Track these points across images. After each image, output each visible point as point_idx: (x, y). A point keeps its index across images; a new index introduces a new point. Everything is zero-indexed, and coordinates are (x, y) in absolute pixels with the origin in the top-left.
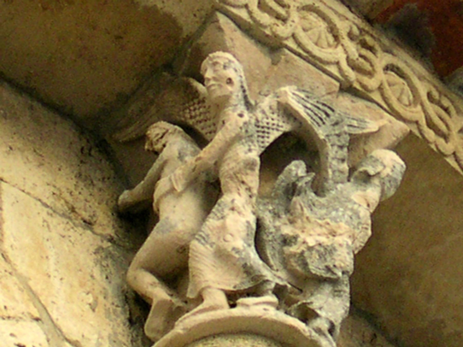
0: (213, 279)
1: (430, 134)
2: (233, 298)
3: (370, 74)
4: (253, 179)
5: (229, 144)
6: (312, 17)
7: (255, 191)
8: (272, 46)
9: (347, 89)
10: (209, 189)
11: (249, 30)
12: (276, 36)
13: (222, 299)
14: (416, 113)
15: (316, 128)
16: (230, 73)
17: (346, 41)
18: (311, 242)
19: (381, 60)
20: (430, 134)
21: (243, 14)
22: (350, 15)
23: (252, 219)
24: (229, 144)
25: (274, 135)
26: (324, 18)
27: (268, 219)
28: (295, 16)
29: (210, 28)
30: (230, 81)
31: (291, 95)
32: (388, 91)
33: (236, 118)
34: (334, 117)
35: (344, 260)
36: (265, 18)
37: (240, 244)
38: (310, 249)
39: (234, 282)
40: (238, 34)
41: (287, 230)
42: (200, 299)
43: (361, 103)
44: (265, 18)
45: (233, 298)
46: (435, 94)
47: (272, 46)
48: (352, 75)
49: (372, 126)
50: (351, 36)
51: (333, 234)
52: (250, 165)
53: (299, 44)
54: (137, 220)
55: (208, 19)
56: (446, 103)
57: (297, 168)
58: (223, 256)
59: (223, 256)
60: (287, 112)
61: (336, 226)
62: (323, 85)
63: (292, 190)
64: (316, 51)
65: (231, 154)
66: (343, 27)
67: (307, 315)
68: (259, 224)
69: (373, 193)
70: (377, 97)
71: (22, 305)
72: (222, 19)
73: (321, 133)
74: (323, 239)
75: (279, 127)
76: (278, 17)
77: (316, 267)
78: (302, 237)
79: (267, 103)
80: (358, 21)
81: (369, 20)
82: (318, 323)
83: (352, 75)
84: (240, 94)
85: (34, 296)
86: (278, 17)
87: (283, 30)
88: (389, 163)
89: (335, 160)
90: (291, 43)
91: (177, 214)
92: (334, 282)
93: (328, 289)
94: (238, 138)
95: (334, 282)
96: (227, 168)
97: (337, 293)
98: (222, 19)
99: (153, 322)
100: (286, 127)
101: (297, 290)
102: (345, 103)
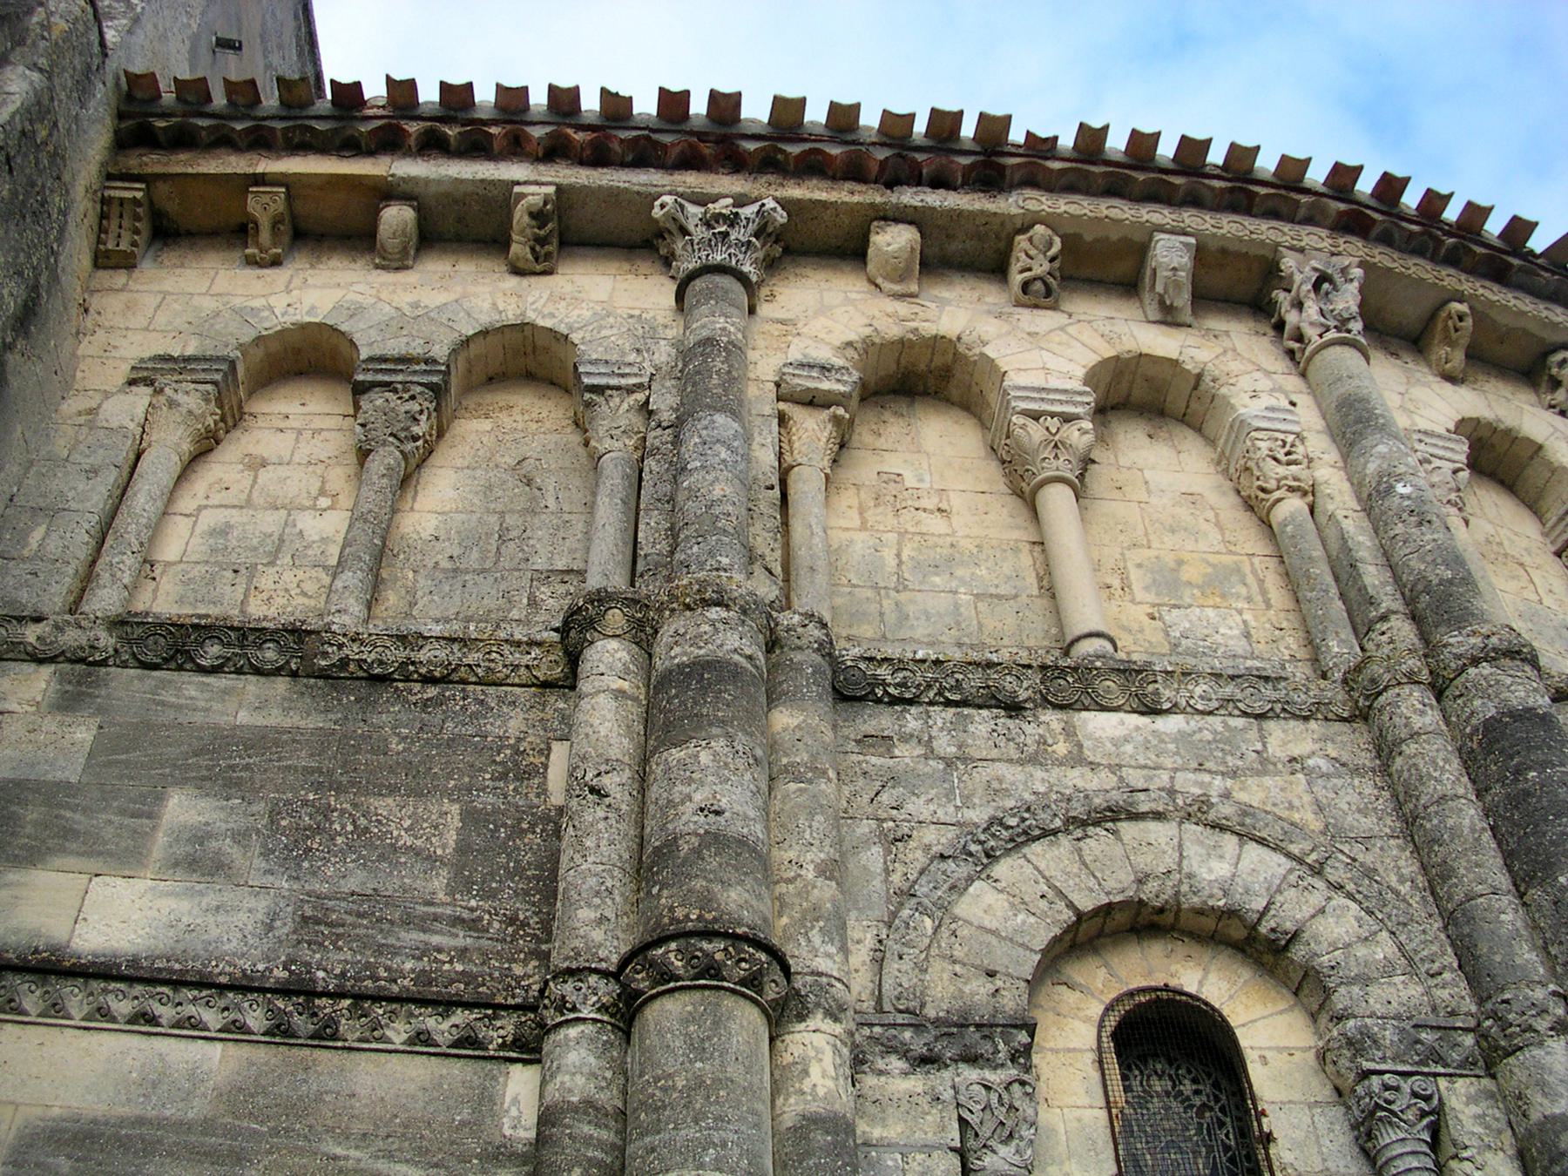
0: (1311, 333)
2: (1321, 336)
4: (1312, 295)
8: (1301, 250)
9: (1333, 254)
10: (1299, 305)
11: (1291, 248)
19: (1341, 241)
31: (1314, 263)
33: (1298, 278)
35: (1355, 309)
45: (1321, 336)
47: (1301, 250)
54: (1280, 326)
55: (1276, 251)
57: (1326, 286)
58: (1312, 324)
59: (1312, 324)
60: (1315, 269)
61: (1347, 299)
62: (1324, 256)
63: (1327, 294)
67: (1349, 331)
69: (1356, 284)
71: (1251, 367)
75: (1315, 276)
77: (1346, 315)
79: (1307, 269)
88: (1357, 272)
91: (1292, 318)
99: (1298, 356)
101: (1343, 324)
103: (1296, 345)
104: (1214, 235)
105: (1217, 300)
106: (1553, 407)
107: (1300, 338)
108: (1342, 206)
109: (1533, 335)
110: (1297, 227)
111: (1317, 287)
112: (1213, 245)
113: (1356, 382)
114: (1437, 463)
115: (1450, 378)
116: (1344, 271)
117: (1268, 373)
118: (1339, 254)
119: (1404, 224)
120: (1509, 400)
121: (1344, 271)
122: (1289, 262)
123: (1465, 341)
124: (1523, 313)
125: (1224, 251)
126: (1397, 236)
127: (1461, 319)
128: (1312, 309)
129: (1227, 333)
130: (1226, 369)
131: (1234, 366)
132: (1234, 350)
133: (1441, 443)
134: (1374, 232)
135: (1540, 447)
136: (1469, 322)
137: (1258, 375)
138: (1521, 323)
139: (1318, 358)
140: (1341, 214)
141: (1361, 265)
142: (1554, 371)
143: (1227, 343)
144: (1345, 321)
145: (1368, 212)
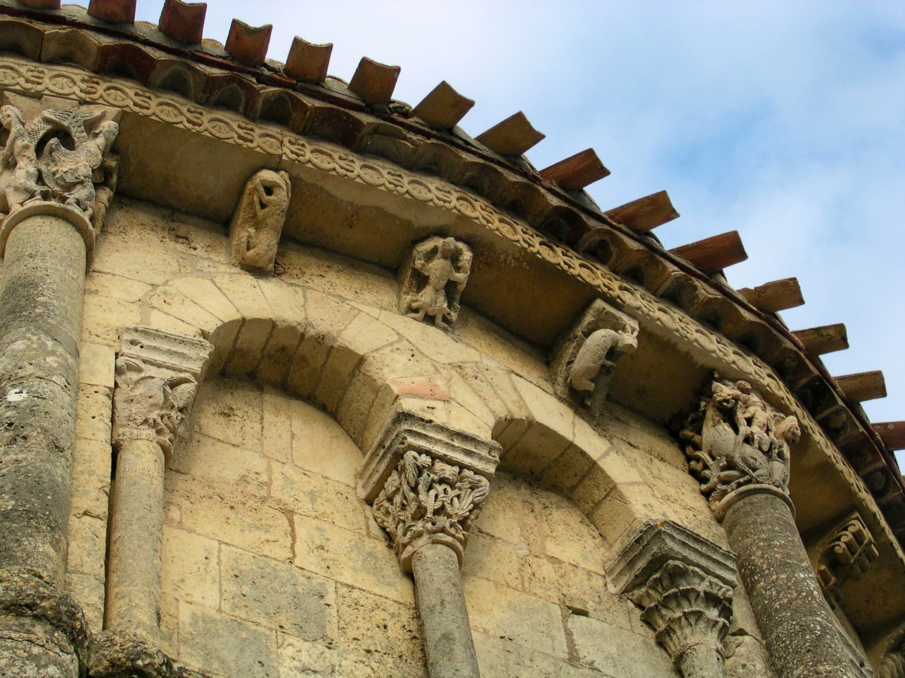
1: (137, 109)
3: (95, 93)
4: (31, 153)
5: (14, 142)
6: (59, 79)
8: (38, 96)
9: (83, 102)
11: (24, 93)
12: (37, 91)
15: (62, 122)
16: (9, 112)
17: (79, 83)
18: (65, 170)
20: (137, 109)
21: (18, 87)
22: (83, 72)
23: (32, 170)
24: (14, 142)
25: (42, 133)
27: (43, 168)
28: (46, 80)
30: (9, 116)
31: (47, 114)
32: (106, 97)
34: (72, 115)
36: (29, 86)
37: (22, 181)
38: (65, 172)
40: (18, 96)
41: (54, 169)
43: (92, 107)
44: (29, 86)
45: (22, 204)
46: (141, 93)
47: (38, 96)
48: (83, 95)
50: (83, 81)
51: (77, 163)
52: (26, 147)
53: (51, 91)
56: (148, 95)
58: (17, 189)
59: (17, 189)
60: (47, 121)
66: (77, 78)
68: (40, 171)
69: (101, 140)
70: (101, 101)
72: (6, 93)
73: (66, 124)
74: (73, 167)
77: (70, 179)
78: (61, 169)
80: (90, 74)
81: (94, 72)
83: (83, 95)
84: (17, 120)
86: (39, 84)
87: (39, 88)
89: (77, 133)
90: (47, 92)
92: (82, 183)
93: (79, 187)
94: (16, 138)
95: (82, 183)
96: (16, 151)
97: (84, 187)
98: (6, 93)
100: (49, 127)
102: (84, 108)
106: (416, 311)
108: (106, 41)
109: (394, 217)
110: (42, 68)
113: (38, 262)
114: (151, 371)
115: (256, 270)
118: (93, 102)
119: (201, 67)
120: (342, 299)
123: (276, 220)
124: (370, 187)
127: (269, 191)
133: (165, 346)
134: (158, 76)
135: (362, 360)
136: (282, 197)
138: (370, 200)
140: (105, 51)
142: (418, 264)
144: (70, 187)
145: (148, 50)
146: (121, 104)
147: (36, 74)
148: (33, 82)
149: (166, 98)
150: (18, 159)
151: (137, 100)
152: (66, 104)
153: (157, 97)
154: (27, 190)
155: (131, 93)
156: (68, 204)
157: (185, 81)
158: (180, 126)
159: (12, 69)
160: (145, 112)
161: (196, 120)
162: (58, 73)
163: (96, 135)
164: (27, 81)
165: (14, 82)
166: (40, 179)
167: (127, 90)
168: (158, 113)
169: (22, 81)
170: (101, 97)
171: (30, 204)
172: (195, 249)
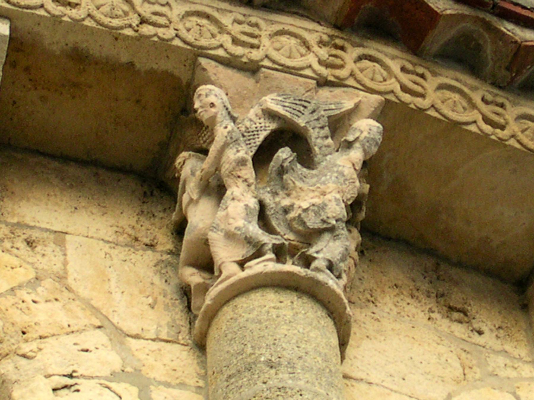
0: (225, 254)
1: (406, 98)
2: (242, 264)
3: (341, 67)
4: (248, 172)
5: (221, 152)
6: (283, 39)
7: (252, 180)
8: (252, 69)
9: (323, 83)
10: (215, 189)
11: (230, 63)
12: (252, 61)
13: (235, 268)
14: (393, 85)
15: (296, 119)
16: (212, 99)
17: (316, 48)
18: (305, 205)
19: (353, 53)
20: (406, 98)
21: (220, 52)
22: (319, 28)
23: (253, 203)
24: (221, 152)
25: (263, 135)
26: (295, 36)
27: (268, 199)
28: (265, 41)
29: (198, 71)
30: (212, 105)
31: (271, 102)
32: (360, 76)
33: (223, 130)
34: (310, 107)
35: (336, 210)
36: (239, 50)
37: (241, 223)
38: (306, 210)
39: (241, 252)
40: (221, 68)
41: (286, 202)
42: (221, 272)
43: (338, 91)
44: (239, 50)
45: (242, 264)
46: (409, 66)
47: (252, 69)
48: (324, 71)
49: (348, 105)
50: (321, 43)
51: (324, 194)
52: (242, 162)
53: (274, 62)
54: (180, 228)
55: (194, 65)
56: (420, 70)
57: (284, 154)
58: (230, 236)
59: (230, 236)
60: (271, 115)
61: (328, 187)
63: (282, 171)
64: (289, 63)
65: (224, 159)
66: (312, 39)
69: (356, 155)
70: (351, 82)
71: (84, 319)
72: (203, 61)
73: (301, 122)
74: (316, 201)
76: (252, 46)
77: (313, 222)
78: (297, 203)
79: (254, 112)
80: (329, 31)
81: (336, 27)
82: (314, 265)
83: (324, 71)
84: (224, 112)
85: (96, 311)
86: (252, 46)
87: (256, 55)
88: (367, 128)
89: (318, 138)
90: (266, 63)
91: (200, 215)
92: (331, 230)
93: (327, 236)
94: (225, 146)
95: (331, 230)
97: (336, 237)
98: (203, 61)
100: (273, 126)
101: (299, 245)
102: (325, 93)
103: (194, 277)
104: (56, 20)
105: (66, 159)
107: (207, 265)
110: (255, 17)
111: (263, 156)
112: (54, 42)
113: (284, 376)
116: (338, 124)
117: (120, 336)
118: (339, 84)
119: (508, 28)
121: (338, 124)
122: (211, 98)
125: (78, 57)
126: (489, 50)
128: (241, 200)
129: (60, 237)
130: (20, 319)
131: (45, 314)
132: (61, 278)
134: (438, 39)
137: (95, 338)
139: (227, 311)
141: (387, 112)
143: (49, 258)
144: (310, 236)
146: (382, 87)
147: (248, 29)
148: (243, 44)
149: (449, 76)
150: (228, 181)
151: (405, 79)
152: (298, 86)
153: (435, 74)
154: (249, 241)
155: (395, 66)
156: (317, 269)
157: (479, 48)
158: (473, 128)
159: (208, 17)
160: (419, 102)
161: (496, 118)
162: (279, 27)
163: (349, 145)
164: (235, 41)
165: (214, 42)
166: (263, 217)
167: (389, 62)
168: (439, 105)
169: (226, 40)
170: (352, 75)
171: (256, 267)
172: (480, 333)
